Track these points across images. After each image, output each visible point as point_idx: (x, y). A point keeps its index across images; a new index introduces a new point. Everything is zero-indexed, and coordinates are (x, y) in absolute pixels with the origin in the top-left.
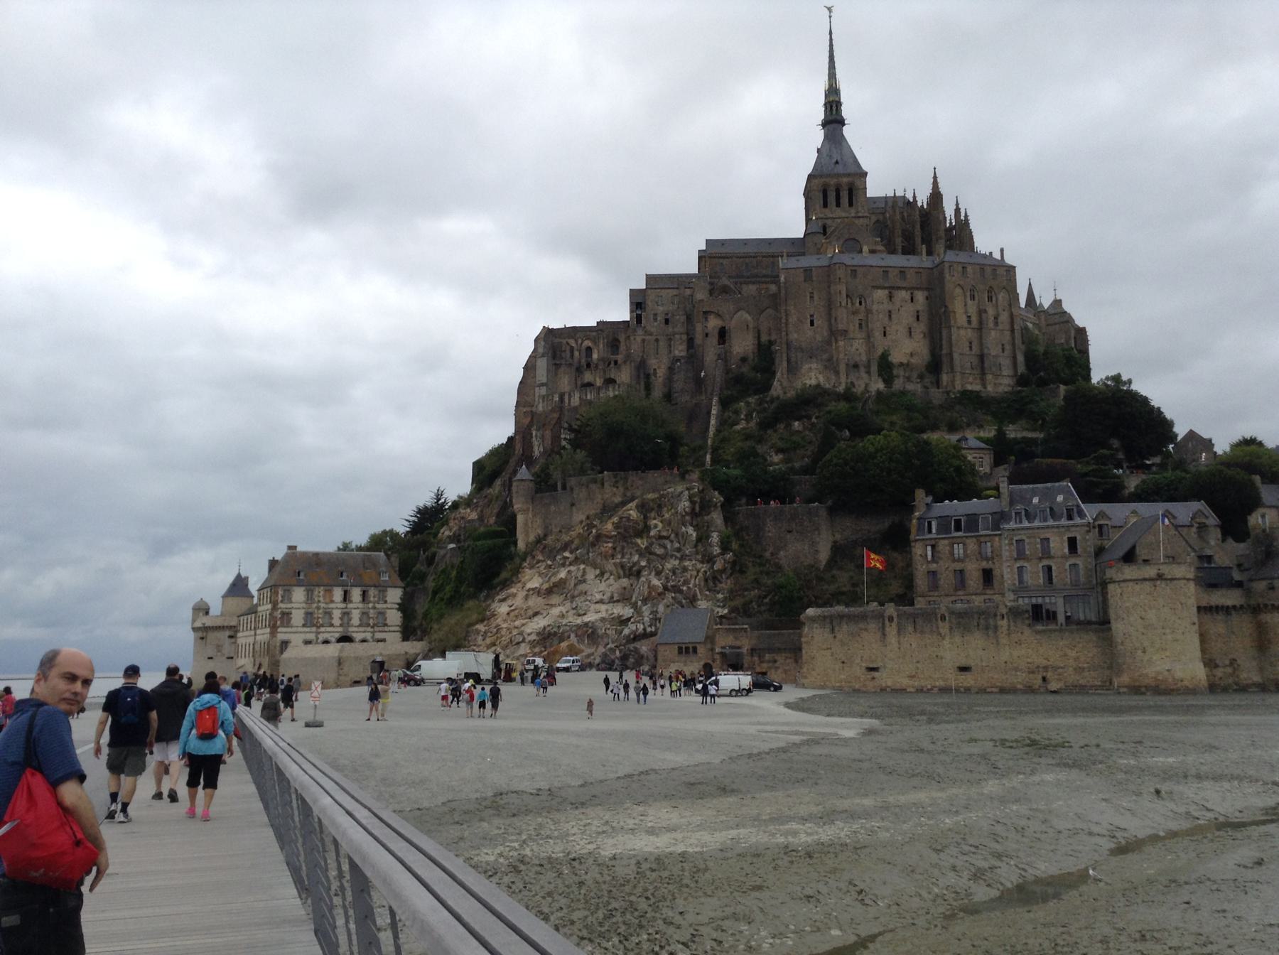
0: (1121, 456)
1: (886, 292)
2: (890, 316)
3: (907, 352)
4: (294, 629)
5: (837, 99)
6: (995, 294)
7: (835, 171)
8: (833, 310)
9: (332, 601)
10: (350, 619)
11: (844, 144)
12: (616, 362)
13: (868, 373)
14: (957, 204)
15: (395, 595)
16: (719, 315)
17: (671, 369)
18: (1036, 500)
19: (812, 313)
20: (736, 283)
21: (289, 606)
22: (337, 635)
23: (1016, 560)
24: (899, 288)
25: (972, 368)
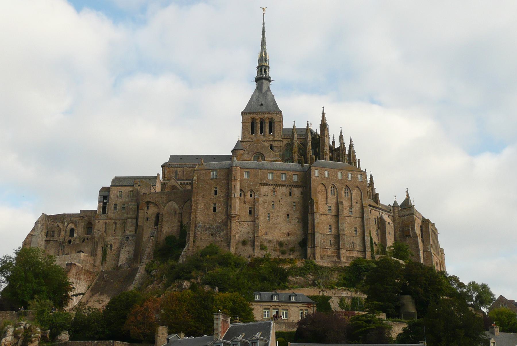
1: (271, 187)
3: (286, 231)
5: (265, 64)
6: (350, 191)
7: (260, 111)
8: (229, 200)
11: (269, 93)
12: (87, 239)
14: (341, 133)
16: (156, 205)
17: (121, 246)
20: (181, 184)
24: (281, 185)
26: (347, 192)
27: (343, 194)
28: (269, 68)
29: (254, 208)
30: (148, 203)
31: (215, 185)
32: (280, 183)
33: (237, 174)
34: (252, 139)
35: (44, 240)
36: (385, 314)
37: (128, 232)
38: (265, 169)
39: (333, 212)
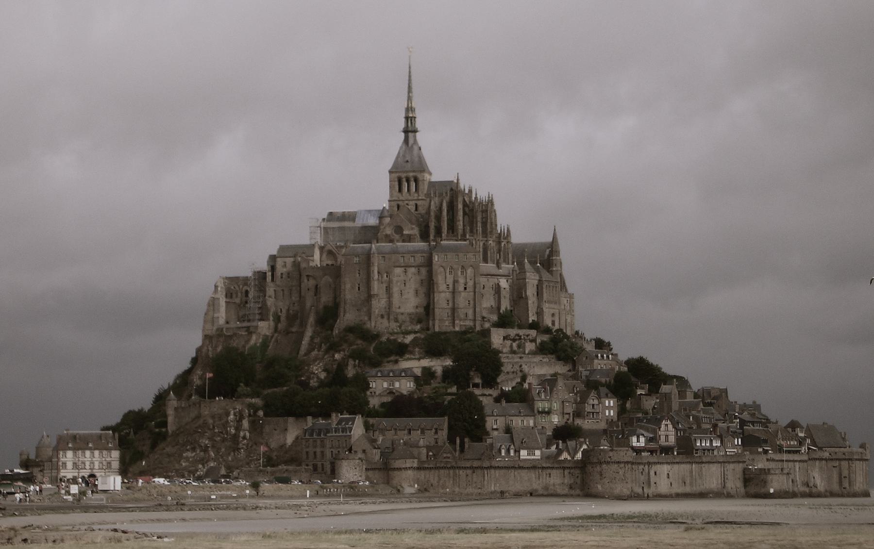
0: (478, 380)
2: (405, 284)
4: (69, 471)
6: (465, 270)
9: (86, 457)
10: (94, 466)
13: (389, 319)
14: (476, 194)
15: (116, 454)
18: (344, 423)
19: (359, 283)
20: (337, 247)
21: (66, 459)
22: (88, 474)
23: (331, 448)
24: (411, 266)
25: (448, 316)
26: (463, 272)
27: (460, 273)
28: (415, 118)
29: (389, 287)
30: (308, 276)
31: (358, 269)
32: (410, 264)
33: (376, 261)
34: (399, 198)
35: (225, 300)
36: (456, 386)
37: (293, 298)
38: (397, 254)
39: (451, 289)
